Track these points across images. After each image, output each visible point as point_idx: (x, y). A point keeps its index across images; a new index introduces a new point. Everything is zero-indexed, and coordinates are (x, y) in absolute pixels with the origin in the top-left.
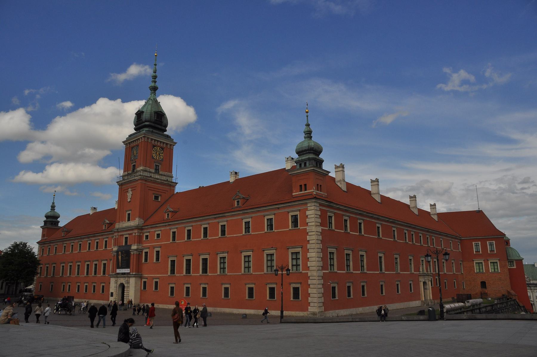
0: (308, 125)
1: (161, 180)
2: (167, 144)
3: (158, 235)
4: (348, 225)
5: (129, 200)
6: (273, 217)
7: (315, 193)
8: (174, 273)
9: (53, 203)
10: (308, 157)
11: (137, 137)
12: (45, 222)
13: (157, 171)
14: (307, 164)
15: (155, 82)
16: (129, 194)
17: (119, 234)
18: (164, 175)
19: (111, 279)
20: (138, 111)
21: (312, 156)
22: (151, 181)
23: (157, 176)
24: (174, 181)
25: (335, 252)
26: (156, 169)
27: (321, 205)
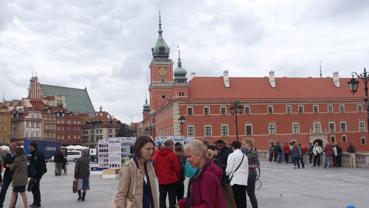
2: (168, 65)
7: (177, 98)
9: (146, 99)
18: (168, 83)
22: (159, 88)
23: (163, 85)
25: (194, 127)
26: (163, 81)
27: (179, 103)
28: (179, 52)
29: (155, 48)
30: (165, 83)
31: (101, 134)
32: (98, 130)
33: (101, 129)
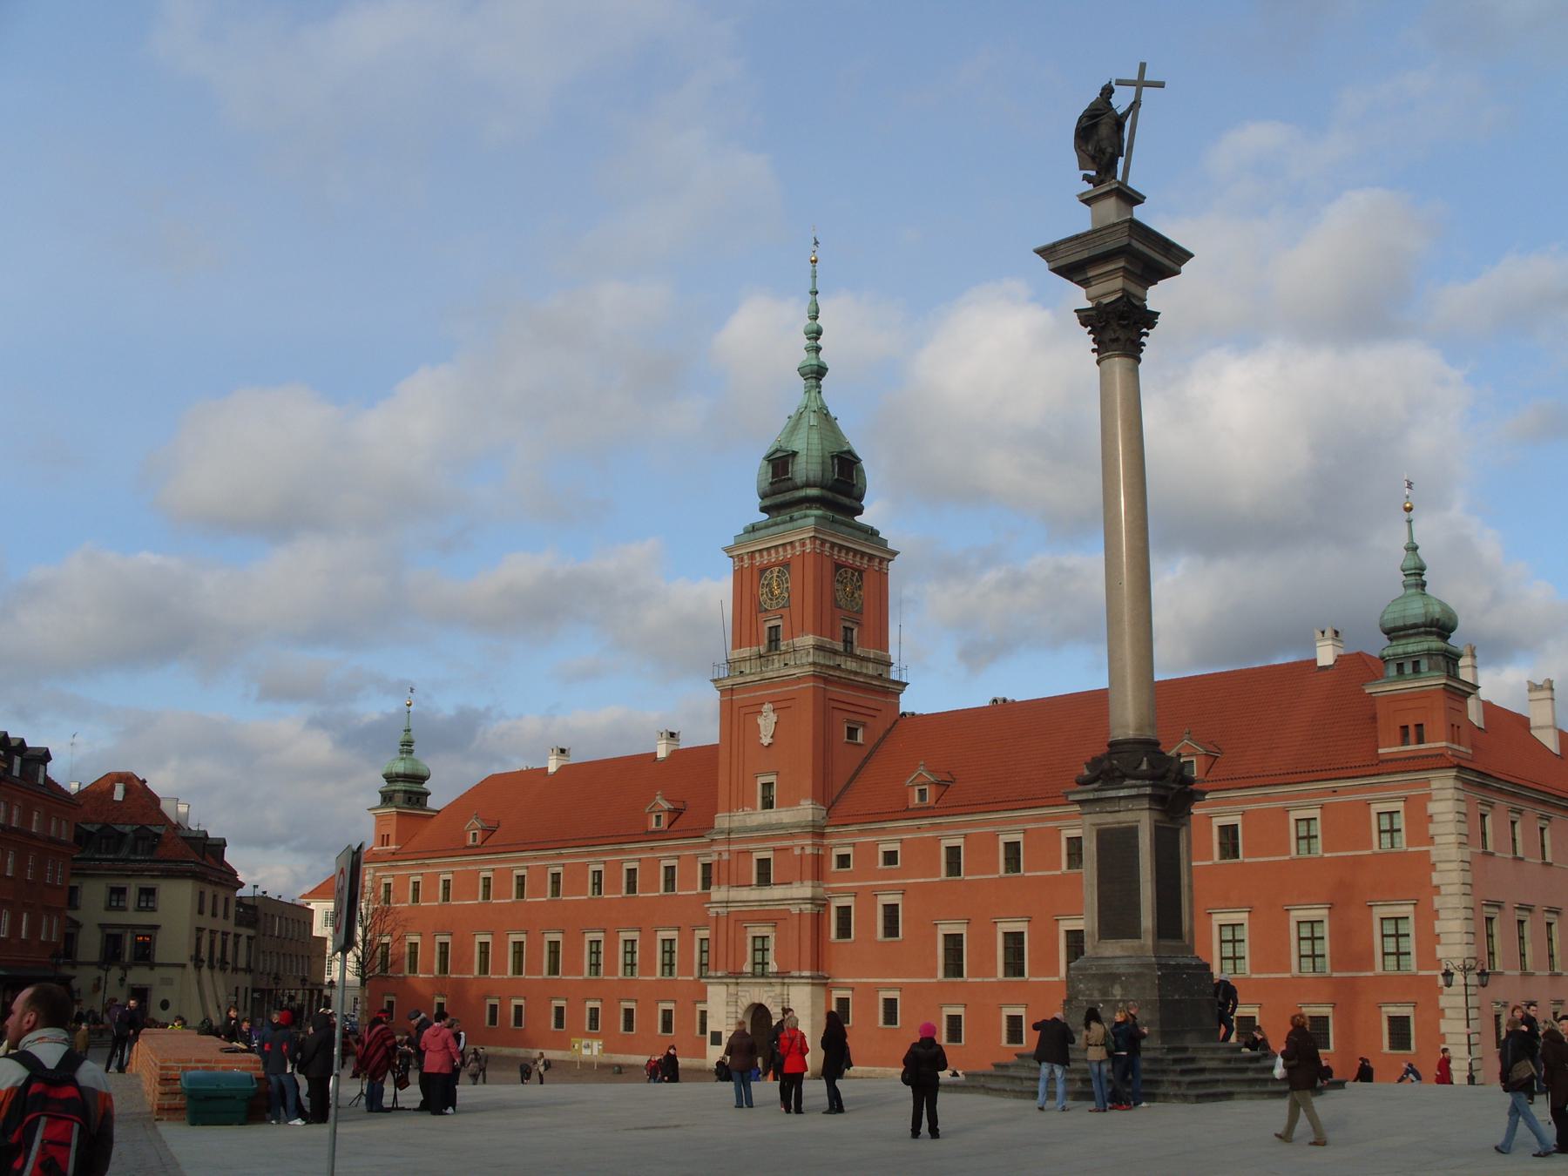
0: (1412, 549)
1: (866, 675)
2: (871, 557)
3: (890, 857)
4: (1518, 838)
5: (766, 741)
6: (1316, 813)
8: (959, 972)
10: (1425, 646)
11: (783, 537)
12: (387, 798)
13: (848, 642)
14: (1424, 666)
15: (818, 349)
16: (767, 723)
17: (734, 847)
19: (710, 988)
20: (777, 451)
21: (1434, 643)
22: (839, 682)
23: (851, 665)
24: (894, 676)
27: (1466, 782)
28: (1409, 510)
29: (815, 453)
30: (849, 653)
31: (145, 919)
32: (119, 892)
33: (148, 883)
